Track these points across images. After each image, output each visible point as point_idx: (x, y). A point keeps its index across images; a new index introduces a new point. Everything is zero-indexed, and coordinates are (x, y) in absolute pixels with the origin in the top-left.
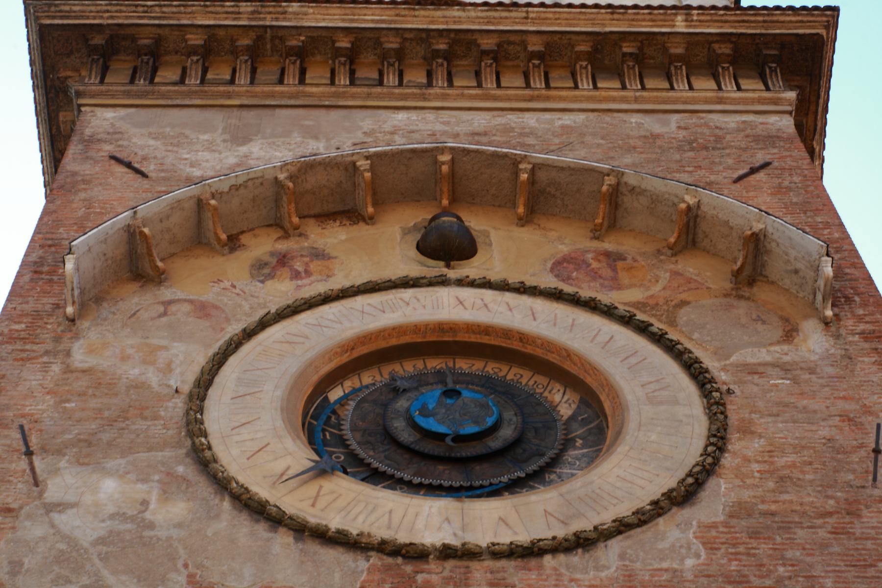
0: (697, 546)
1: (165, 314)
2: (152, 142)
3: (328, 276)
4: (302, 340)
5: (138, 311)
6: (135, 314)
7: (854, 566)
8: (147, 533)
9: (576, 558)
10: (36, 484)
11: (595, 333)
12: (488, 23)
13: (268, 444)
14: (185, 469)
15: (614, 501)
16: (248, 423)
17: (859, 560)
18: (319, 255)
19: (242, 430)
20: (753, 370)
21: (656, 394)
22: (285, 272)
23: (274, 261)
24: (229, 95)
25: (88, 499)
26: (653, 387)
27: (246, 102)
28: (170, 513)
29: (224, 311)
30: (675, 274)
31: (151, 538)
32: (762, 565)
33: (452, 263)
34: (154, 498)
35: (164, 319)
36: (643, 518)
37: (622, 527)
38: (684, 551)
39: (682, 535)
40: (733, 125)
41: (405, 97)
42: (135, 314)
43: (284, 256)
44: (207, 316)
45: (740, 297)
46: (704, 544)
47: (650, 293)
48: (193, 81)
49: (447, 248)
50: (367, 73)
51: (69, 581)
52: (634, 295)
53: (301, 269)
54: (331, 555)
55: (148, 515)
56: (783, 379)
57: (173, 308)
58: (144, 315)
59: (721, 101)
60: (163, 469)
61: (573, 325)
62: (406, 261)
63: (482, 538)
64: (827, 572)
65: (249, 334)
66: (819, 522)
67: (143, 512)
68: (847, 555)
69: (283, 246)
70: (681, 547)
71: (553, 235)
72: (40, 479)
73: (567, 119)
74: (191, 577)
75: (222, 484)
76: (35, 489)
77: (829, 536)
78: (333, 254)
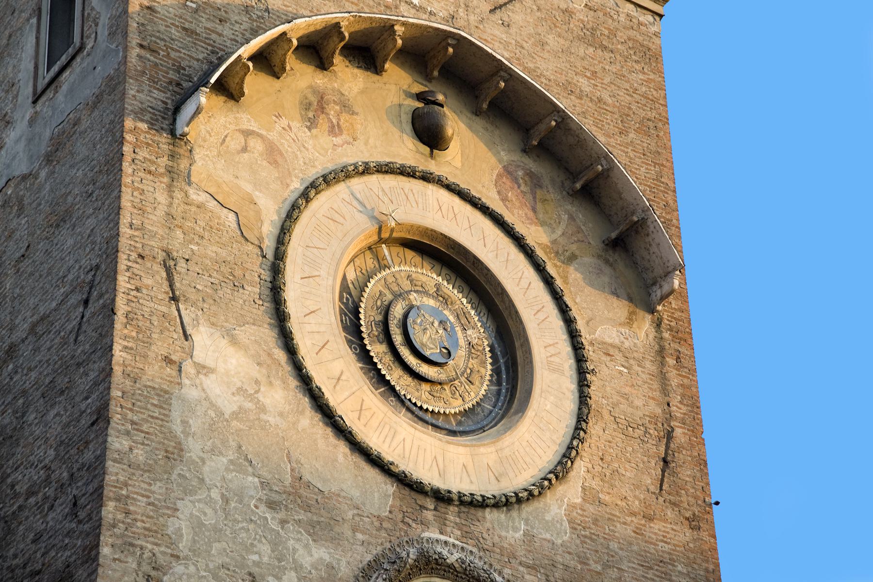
0: (566, 524)
1: (245, 149)
3: (355, 140)
4: (341, 220)
5: (226, 136)
6: (224, 140)
7: (642, 566)
8: (263, 417)
10: (186, 339)
11: (520, 274)
13: (328, 341)
15: (525, 466)
16: (314, 312)
17: (645, 561)
18: (346, 107)
19: (311, 319)
20: (608, 350)
21: (552, 359)
23: (314, 100)
25: (221, 367)
26: (552, 350)
29: (286, 161)
30: (572, 218)
31: (266, 422)
32: (597, 551)
33: (435, 151)
34: (263, 380)
35: (246, 155)
38: (558, 526)
39: (559, 511)
42: (224, 140)
43: (322, 98)
44: (274, 163)
46: (569, 522)
47: (555, 236)
51: (221, 453)
53: (334, 121)
54: (372, 474)
55: (260, 396)
56: (623, 366)
57: (253, 142)
60: (265, 348)
61: (507, 260)
63: (456, 482)
64: (629, 567)
66: (629, 519)
67: (257, 392)
68: (640, 555)
70: (557, 522)
71: (497, 132)
72: (188, 333)
74: (292, 470)
75: (305, 381)
76: (186, 343)
77: (633, 534)
78: (356, 109)
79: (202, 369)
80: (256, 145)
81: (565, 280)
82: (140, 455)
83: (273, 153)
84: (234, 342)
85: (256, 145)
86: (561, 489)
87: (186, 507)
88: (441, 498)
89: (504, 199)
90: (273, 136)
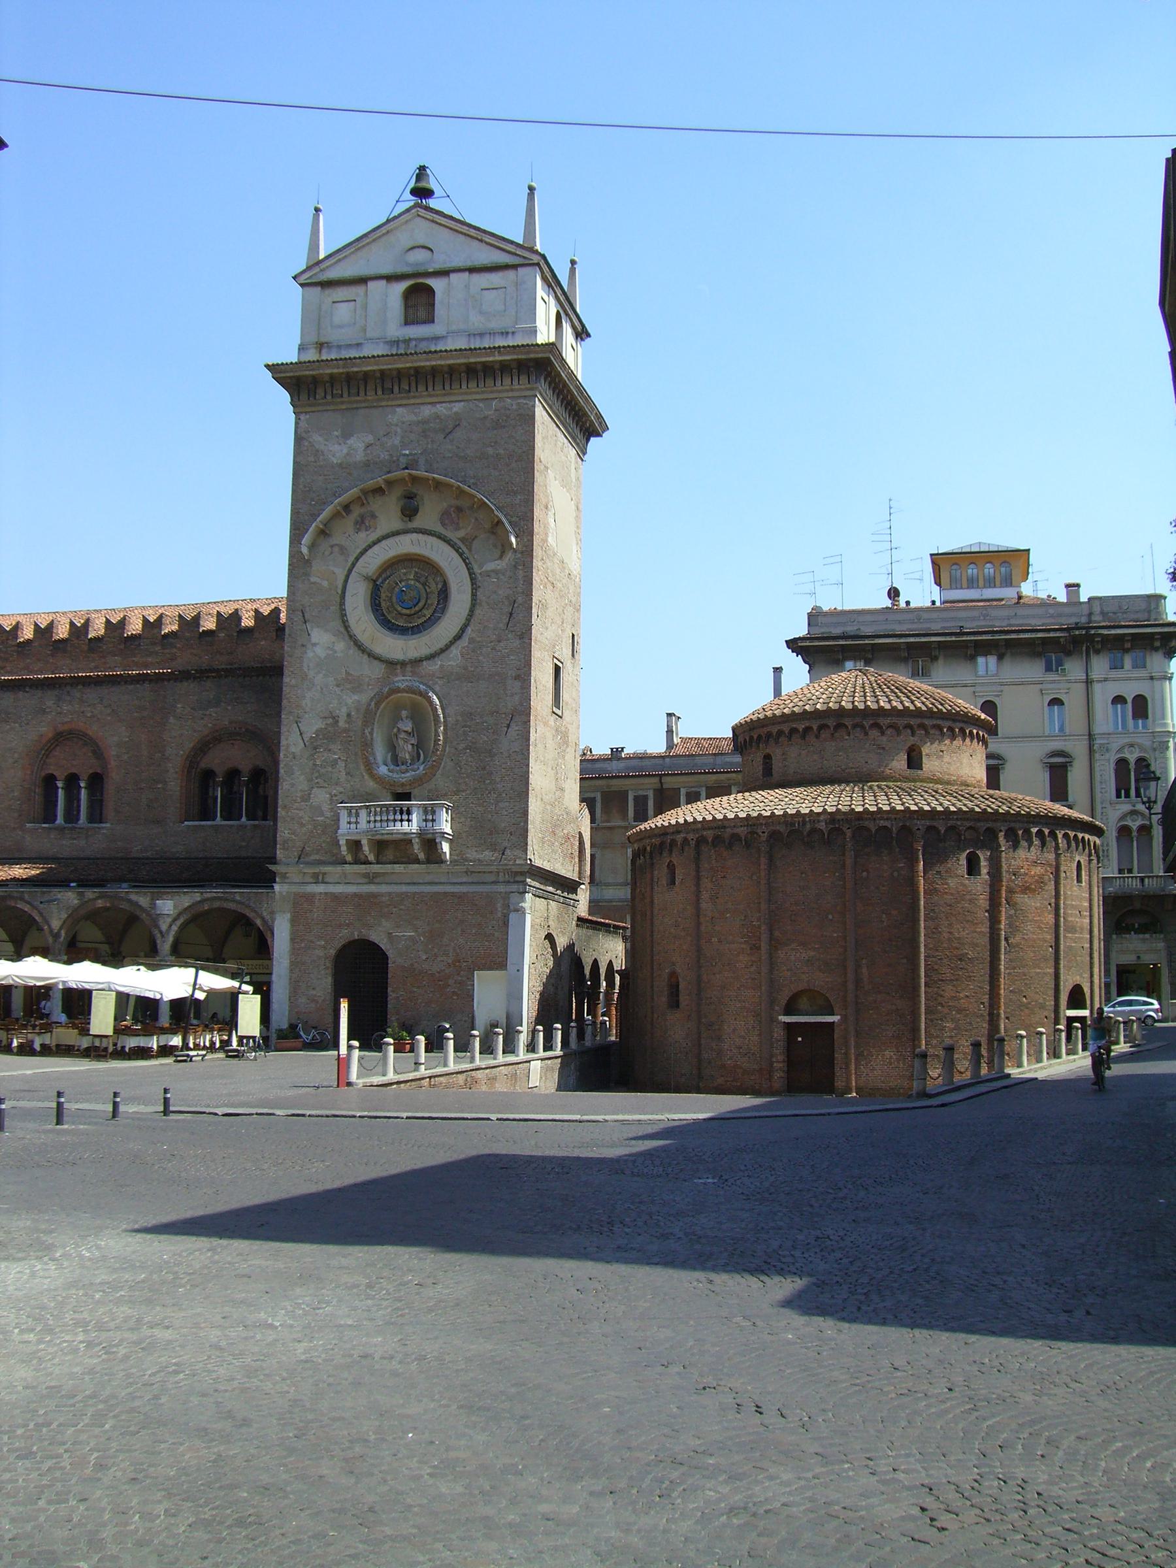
2: (320, 439)
9: (430, 662)
12: (427, 360)
14: (342, 629)
18: (373, 516)
20: (488, 574)
22: (363, 527)
24: (342, 403)
27: (349, 406)
28: (341, 646)
36: (447, 647)
37: (443, 651)
40: (514, 407)
41: (402, 398)
45: (493, 533)
48: (329, 397)
49: (410, 511)
50: (388, 385)
52: (461, 533)
54: (376, 662)
58: (327, 553)
59: (512, 390)
62: (396, 524)
65: (353, 565)
69: (362, 510)
73: (457, 407)
75: (352, 637)
79: (315, 645)
80: (336, 549)
81: (470, 550)
82: (293, 682)
83: (343, 550)
84: (326, 631)
85: (336, 549)
86: (458, 642)
87: (309, 695)
88: (403, 664)
89: (443, 524)
90: (343, 543)
